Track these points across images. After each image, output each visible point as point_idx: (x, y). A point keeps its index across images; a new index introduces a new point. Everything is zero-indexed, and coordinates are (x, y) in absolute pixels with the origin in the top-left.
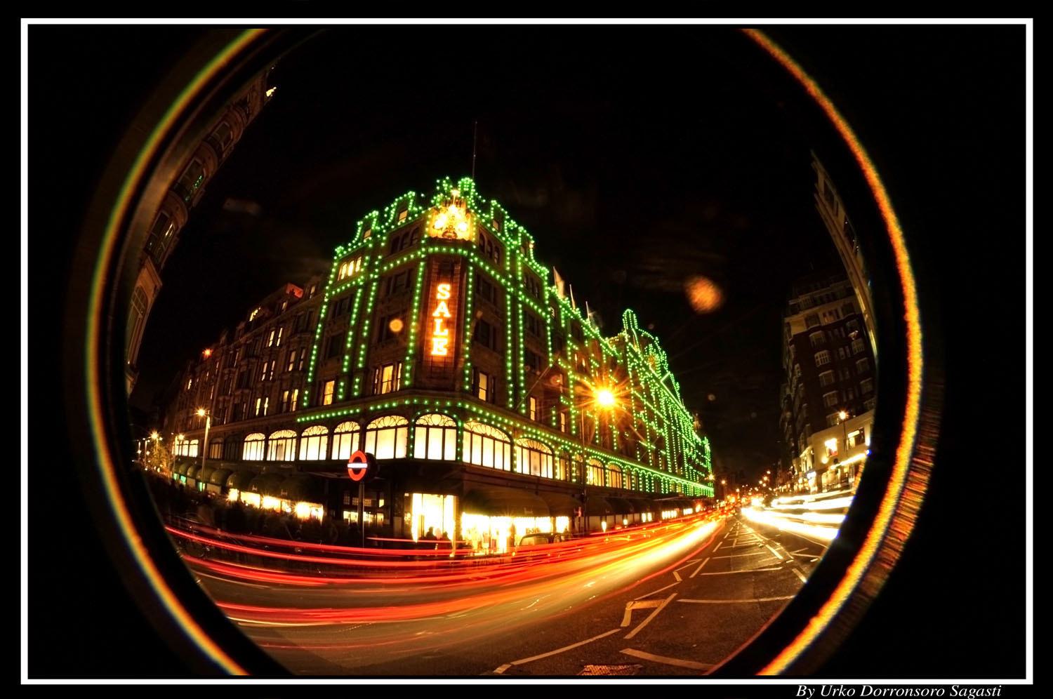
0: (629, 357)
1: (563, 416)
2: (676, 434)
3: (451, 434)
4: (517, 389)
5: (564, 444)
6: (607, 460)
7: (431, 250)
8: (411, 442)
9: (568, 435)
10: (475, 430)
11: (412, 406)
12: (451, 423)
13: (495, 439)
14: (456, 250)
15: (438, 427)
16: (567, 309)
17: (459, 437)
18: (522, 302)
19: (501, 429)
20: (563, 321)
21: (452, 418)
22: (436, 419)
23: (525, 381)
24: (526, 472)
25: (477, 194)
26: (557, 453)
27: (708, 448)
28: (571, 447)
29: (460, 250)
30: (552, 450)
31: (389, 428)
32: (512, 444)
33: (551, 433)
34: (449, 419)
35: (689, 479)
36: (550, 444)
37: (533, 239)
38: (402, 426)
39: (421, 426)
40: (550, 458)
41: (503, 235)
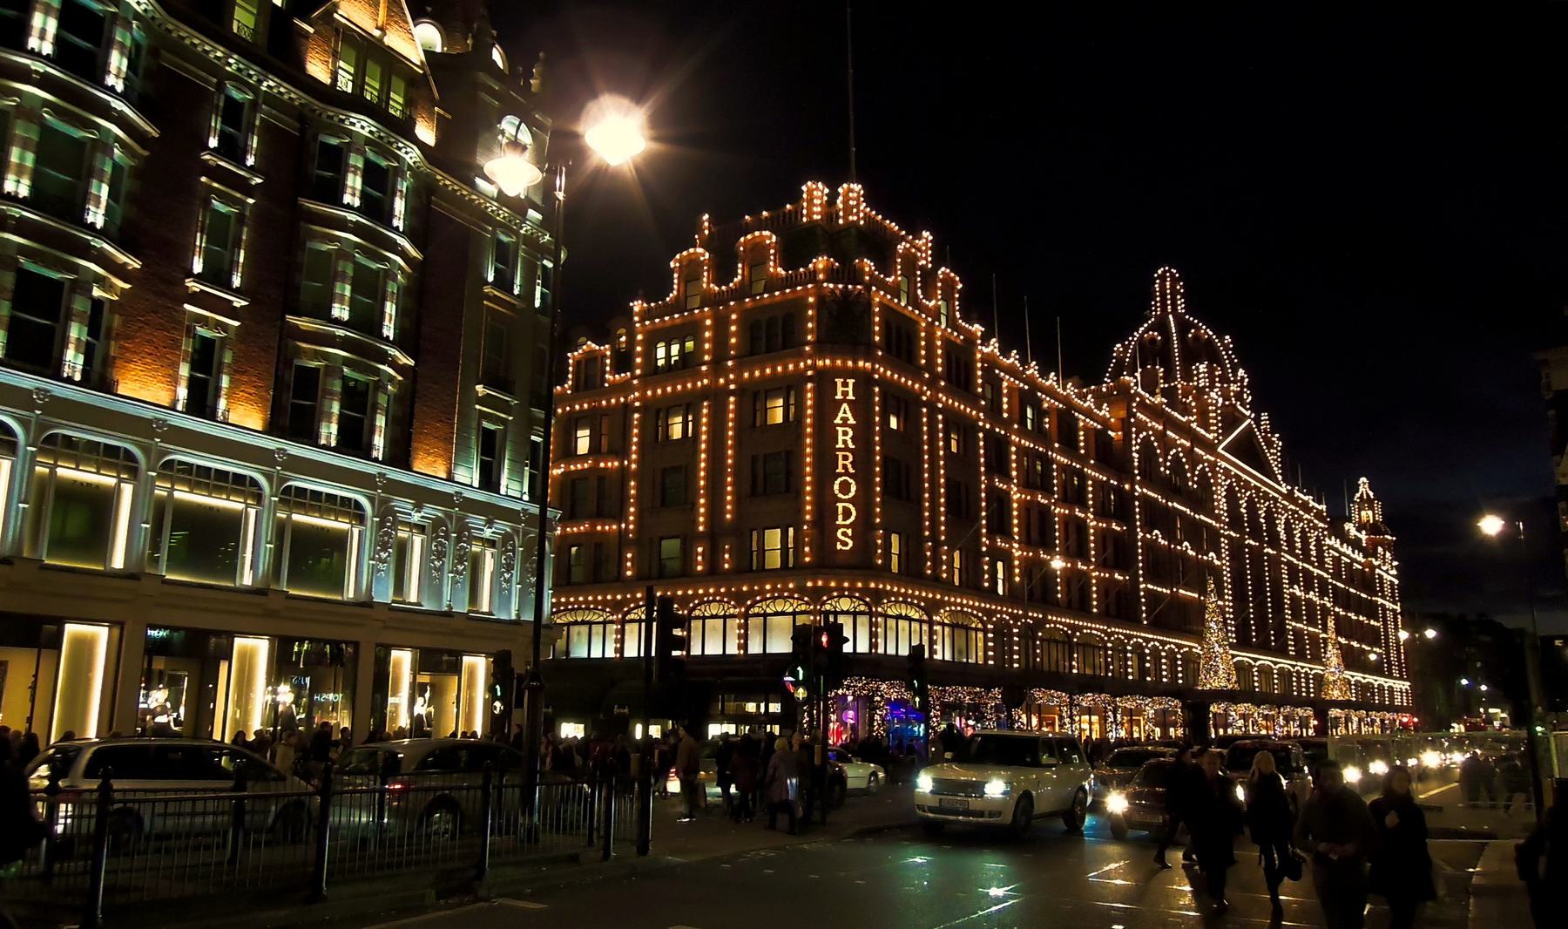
1: (1000, 565)
2: (1256, 554)
3: (863, 621)
5: (1001, 612)
9: (1013, 597)
10: (889, 612)
11: (815, 588)
12: (862, 608)
13: (910, 620)
14: (855, 362)
16: (1011, 371)
19: (918, 606)
23: (947, 533)
24: (948, 657)
25: (868, 209)
27: (1388, 572)
28: (1012, 616)
29: (861, 364)
30: (984, 624)
31: (783, 613)
32: (931, 623)
35: (1300, 656)
36: (980, 615)
37: (961, 281)
40: (980, 635)
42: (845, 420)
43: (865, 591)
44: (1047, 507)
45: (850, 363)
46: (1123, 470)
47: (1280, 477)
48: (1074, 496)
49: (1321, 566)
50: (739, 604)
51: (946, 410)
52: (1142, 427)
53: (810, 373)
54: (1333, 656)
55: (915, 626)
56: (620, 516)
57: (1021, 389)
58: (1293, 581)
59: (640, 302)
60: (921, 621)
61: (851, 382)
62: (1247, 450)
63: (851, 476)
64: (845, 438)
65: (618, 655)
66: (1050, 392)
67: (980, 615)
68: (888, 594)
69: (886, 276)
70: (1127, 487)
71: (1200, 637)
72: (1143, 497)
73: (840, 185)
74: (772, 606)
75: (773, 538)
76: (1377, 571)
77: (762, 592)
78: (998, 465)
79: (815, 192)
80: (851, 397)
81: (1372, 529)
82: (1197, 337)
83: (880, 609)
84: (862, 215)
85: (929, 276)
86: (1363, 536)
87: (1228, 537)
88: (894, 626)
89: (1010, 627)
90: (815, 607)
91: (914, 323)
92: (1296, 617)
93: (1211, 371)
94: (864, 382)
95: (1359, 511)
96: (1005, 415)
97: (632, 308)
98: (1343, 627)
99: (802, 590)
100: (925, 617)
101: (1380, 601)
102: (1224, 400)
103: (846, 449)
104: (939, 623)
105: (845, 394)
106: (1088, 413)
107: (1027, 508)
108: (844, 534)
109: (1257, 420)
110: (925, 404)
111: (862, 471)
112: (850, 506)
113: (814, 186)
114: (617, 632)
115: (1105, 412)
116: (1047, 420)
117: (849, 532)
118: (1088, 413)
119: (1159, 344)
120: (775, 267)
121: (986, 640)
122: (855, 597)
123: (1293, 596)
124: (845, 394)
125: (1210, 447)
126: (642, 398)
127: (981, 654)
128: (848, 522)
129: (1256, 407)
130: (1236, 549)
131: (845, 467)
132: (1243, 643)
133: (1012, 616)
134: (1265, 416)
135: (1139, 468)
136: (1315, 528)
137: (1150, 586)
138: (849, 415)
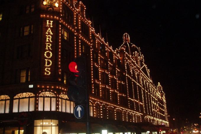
0: (126, 59)
2: (147, 94)
3: (54, 100)
5: (97, 101)
8: (36, 105)
10: (63, 97)
12: (54, 95)
14: (53, 17)
15: (48, 97)
17: (57, 101)
18: (80, 39)
22: (47, 94)
28: (100, 102)
30: (93, 104)
31: (25, 98)
38: (32, 97)
39: (41, 97)
41: (73, 7)
42: (49, 34)
43: (55, 90)
61: (52, 22)
67: (92, 101)
88: (65, 102)
89: (100, 106)
94: (56, 23)
101: (164, 106)
103: (49, 42)
111: (54, 49)
115: (119, 55)
116: (106, 53)
117: (49, 69)
121: (93, 109)
122: (51, 92)
128: (49, 66)
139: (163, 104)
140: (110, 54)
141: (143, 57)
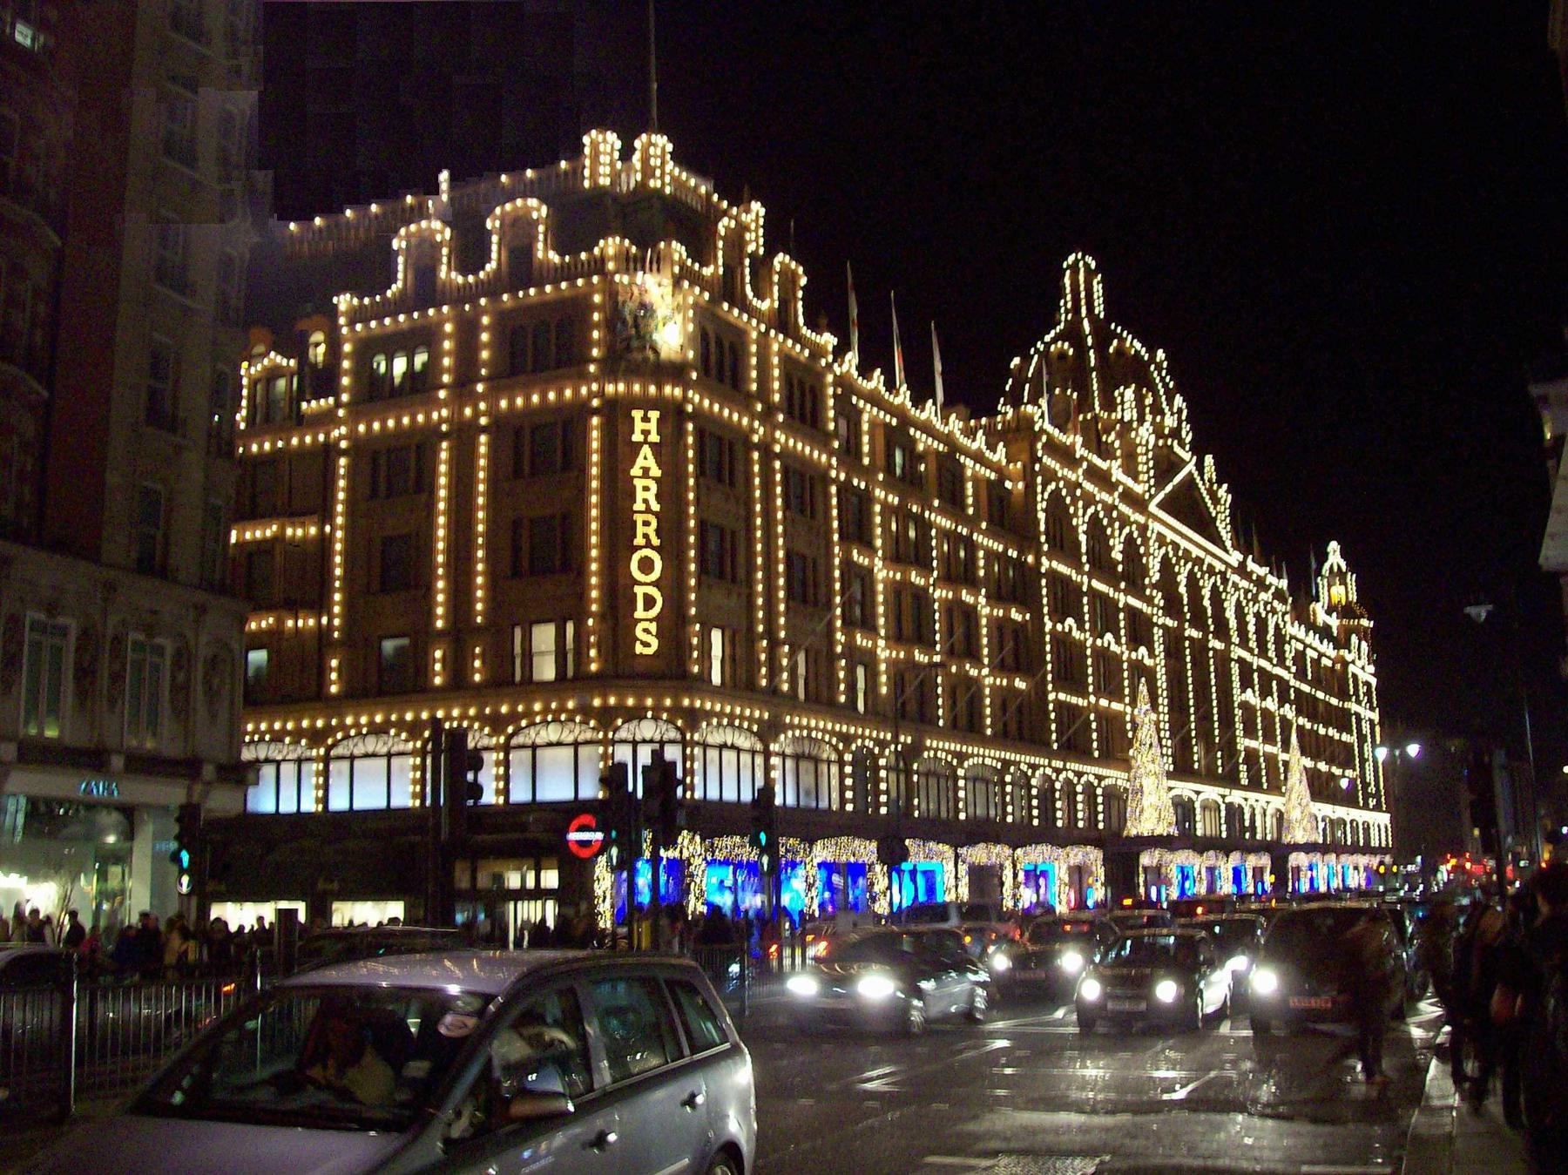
1: (860, 672)
2: (1200, 648)
4: (774, 644)
6: (961, 757)
7: (610, 389)
9: (875, 715)
11: (605, 708)
13: (739, 750)
14: (660, 388)
16: (874, 399)
19: (749, 730)
20: (866, 439)
21: (674, 724)
24: (791, 801)
26: (848, 757)
27: (1363, 670)
28: (878, 742)
29: (668, 390)
32: (767, 754)
33: (837, 718)
34: (670, 726)
35: (1254, 785)
40: (834, 769)
42: (646, 471)
43: (676, 711)
44: (925, 589)
45: (652, 389)
46: (1022, 533)
47: (1228, 544)
48: (959, 573)
49: (1281, 662)
50: (496, 731)
51: (785, 455)
52: (1050, 476)
53: (595, 403)
54: (1297, 784)
55: (746, 758)
56: (320, 605)
57: (887, 426)
58: (1246, 683)
59: (348, 296)
60: (753, 752)
61: (654, 415)
62: (1187, 507)
63: (653, 548)
64: (646, 494)
65: (320, 807)
66: (927, 429)
68: (708, 715)
69: (702, 266)
70: (1030, 559)
71: (1125, 764)
72: (1053, 575)
73: (637, 136)
74: (543, 733)
75: (544, 636)
76: (1351, 668)
77: (529, 714)
78: (858, 532)
79: (602, 144)
80: (654, 437)
81: (1345, 611)
82: (1120, 351)
83: (696, 737)
84: (667, 179)
85: (761, 266)
86: (1334, 622)
87: (1164, 627)
90: (606, 735)
91: (740, 334)
92: (1250, 732)
93: (1139, 399)
94: (673, 415)
95: (1329, 586)
96: (866, 461)
97: (336, 306)
98: (1312, 746)
99: (586, 711)
100: (759, 746)
102: (1157, 439)
103: (648, 510)
104: (777, 754)
105: (646, 433)
106: (978, 458)
107: (898, 590)
108: (646, 631)
109: (1200, 466)
110: (757, 447)
112: (655, 592)
113: (600, 137)
114: (318, 774)
115: (1000, 455)
117: (653, 627)
118: (978, 458)
119: (1070, 361)
120: (546, 250)
121: (842, 776)
123: (1245, 706)
124: (646, 433)
125: (1139, 504)
126: (352, 436)
127: (835, 795)
129: (1198, 450)
130: (1174, 642)
131: (646, 536)
132: (1182, 769)
133: (878, 742)
134: (1209, 460)
135: (1047, 533)
136: (1274, 611)
137: (1062, 696)
138: (651, 463)
139: (1344, 695)
140: (940, 468)
141: (1180, 411)
